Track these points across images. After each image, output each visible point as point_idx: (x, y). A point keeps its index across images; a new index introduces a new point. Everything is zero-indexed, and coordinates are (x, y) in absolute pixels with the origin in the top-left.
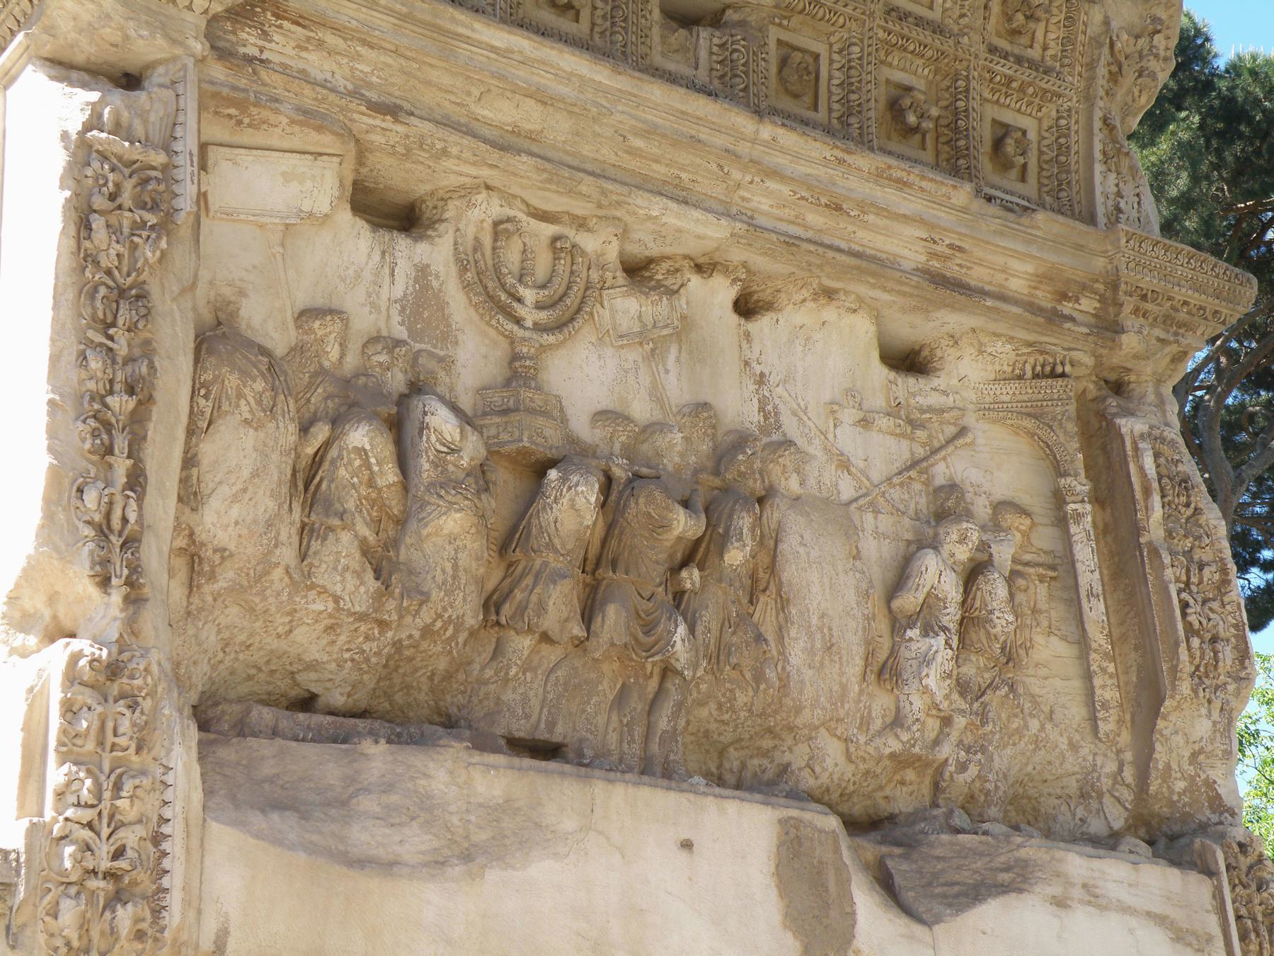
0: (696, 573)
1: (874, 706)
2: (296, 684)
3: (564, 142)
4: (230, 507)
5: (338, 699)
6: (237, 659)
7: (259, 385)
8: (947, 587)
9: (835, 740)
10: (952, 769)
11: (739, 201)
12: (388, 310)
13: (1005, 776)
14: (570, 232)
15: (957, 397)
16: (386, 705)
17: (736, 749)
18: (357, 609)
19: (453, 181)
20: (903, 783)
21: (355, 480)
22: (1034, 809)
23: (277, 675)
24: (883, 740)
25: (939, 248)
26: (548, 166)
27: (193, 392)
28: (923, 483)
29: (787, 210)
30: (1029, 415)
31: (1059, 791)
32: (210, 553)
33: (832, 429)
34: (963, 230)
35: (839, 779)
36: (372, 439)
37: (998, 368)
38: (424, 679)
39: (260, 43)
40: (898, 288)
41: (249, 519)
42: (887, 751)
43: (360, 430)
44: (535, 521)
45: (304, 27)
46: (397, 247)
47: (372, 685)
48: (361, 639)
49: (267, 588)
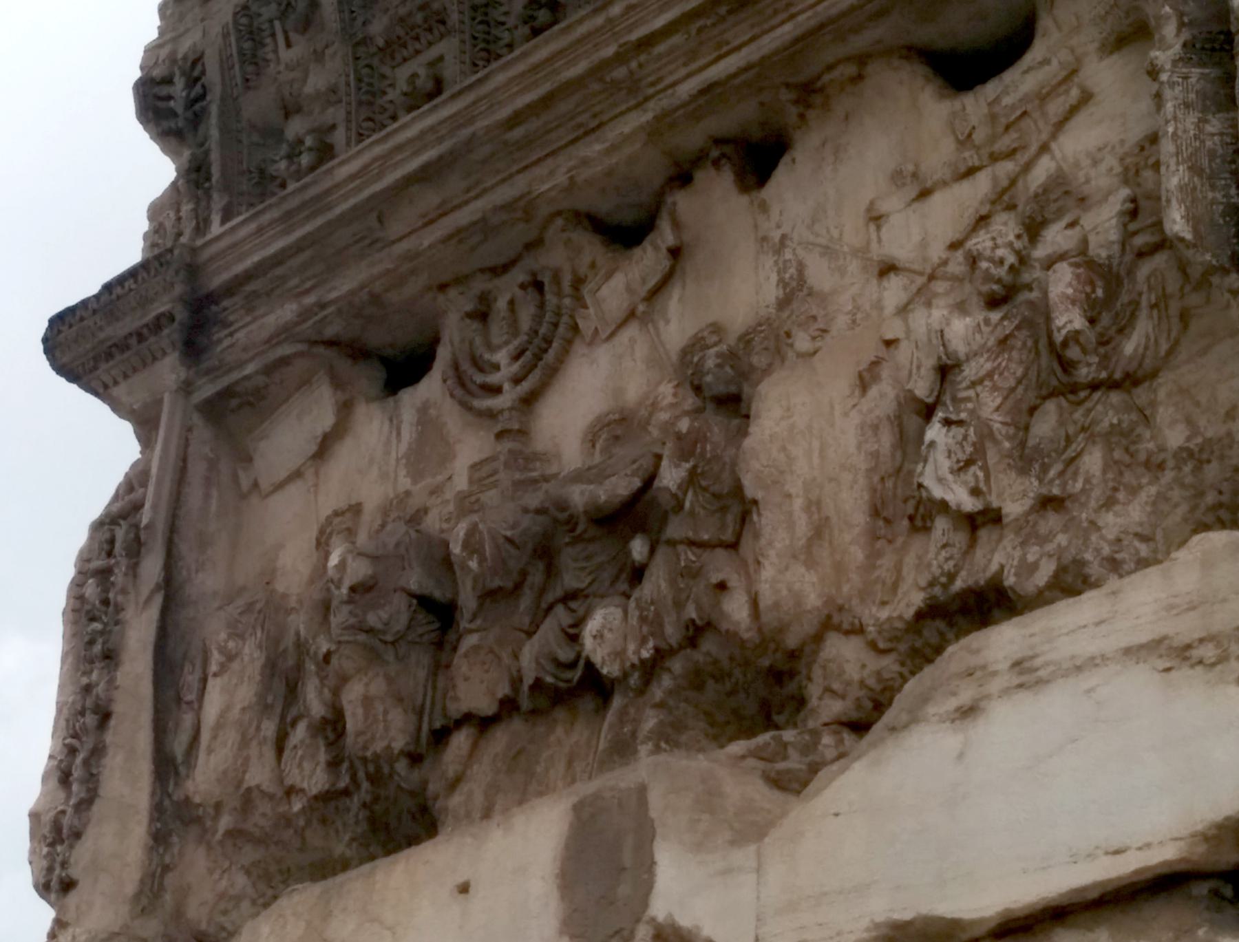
11: (651, 91)
12: (396, 472)
14: (530, 263)
17: (779, 713)
33: (874, 236)
39: (226, 332)
42: (909, 613)
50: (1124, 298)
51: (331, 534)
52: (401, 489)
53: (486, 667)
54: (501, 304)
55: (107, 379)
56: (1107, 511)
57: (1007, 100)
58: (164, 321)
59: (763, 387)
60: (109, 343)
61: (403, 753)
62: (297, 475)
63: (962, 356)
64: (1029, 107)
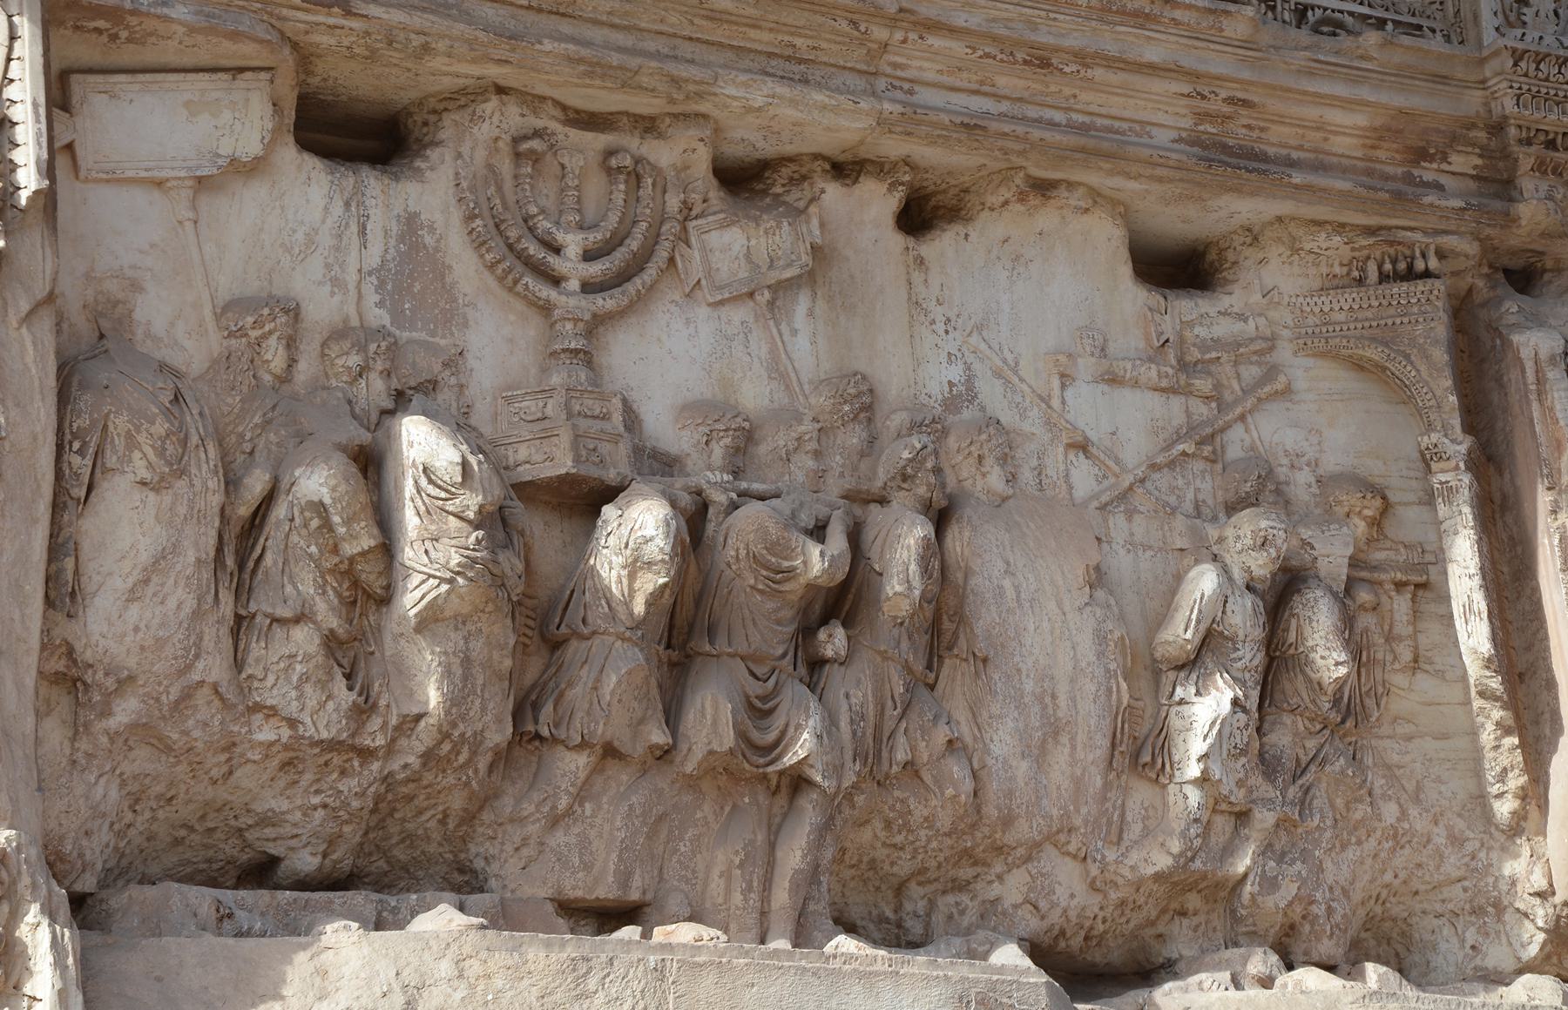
0: (840, 633)
1: (1130, 804)
2: (247, 845)
3: (609, 13)
4: (126, 608)
5: (306, 861)
7: (160, 427)
9: (1067, 859)
13: (1345, 892)
14: (633, 142)
15: (1262, 321)
16: (382, 864)
17: (920, 884)
18: (325, 735)
19: (447, 83)
20: (1183, 913)
21: (313, 549)
22: (1403, 934)
23: (219, 835)
24: (1144, 854)
25: (1215, 106)
26: (585, 52)
27: (60, 448)
28: (1206, 459)
29: (965, 75)
30: (1373, 339)
31: (1439, 907)
32: (100, 674)
33: (1057, 391)
34: (1246, 75)
35: (1078, 916)
36: (333, 490)
37: (1325, 270)
38: (433, 824)
40: (1149, 171)
41: (157, 621)
42: (1150, 870)
43: (315, 477)
44: (589, 583)
46: (368, 192)
47: (358, 839)
48: (335, 775)
49: (188, 717)
51: (271, 333)
57: (1200, 331)
62: (159, 184)
64: (1225, 357)
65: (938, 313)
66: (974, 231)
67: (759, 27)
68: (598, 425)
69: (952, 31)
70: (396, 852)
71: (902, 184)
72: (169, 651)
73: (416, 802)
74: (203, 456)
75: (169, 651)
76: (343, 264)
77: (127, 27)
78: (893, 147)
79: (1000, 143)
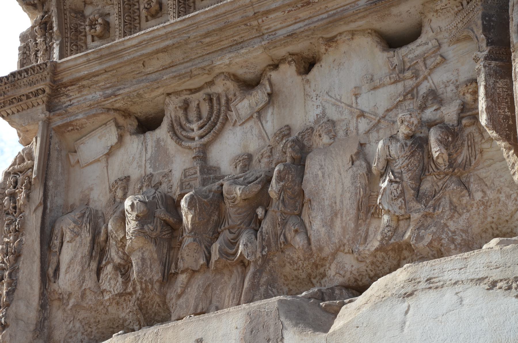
4: (66, 276)
6: (98, 328)
8: (393, 153)
9: (348, 255)
10: (414, 241)
14: (208, 90)
17: (314, 278)
18: (116, 292)
28: (410, 99)
29: (289, 20)
32: (64, 296)
35: (357, 272)
37: (452, 12)
38: (157, 307)
39: (68, 99)
40: (357, 17)
42: (373, 249)
45: (74, 85)
50: (459, 142)
51: (117, 188)
52: (148, 173)
53: (195, 251)
54: (193, 105)
55: (9, 111)
56: (451, 220)
57: (411, 56)
58: (40, 92)
59: (311, 154)
60: (12, 98)
61: (157, 281)
62: (98, 160)
63: (396, 158)
64: (419, 60)
65: (314, 94)
66: (323, 64)
67: (223, 41)
68: (194, 176)
69: (275, 10)
70: (156, 318)
71: (291, 61)
72: (76, 283)
73: (149, 303)
74: (86, 228)
75: (76, 283)
76: (141, 161)
77: (76, 126)
78: (281, 52)
79: (303, 35)
